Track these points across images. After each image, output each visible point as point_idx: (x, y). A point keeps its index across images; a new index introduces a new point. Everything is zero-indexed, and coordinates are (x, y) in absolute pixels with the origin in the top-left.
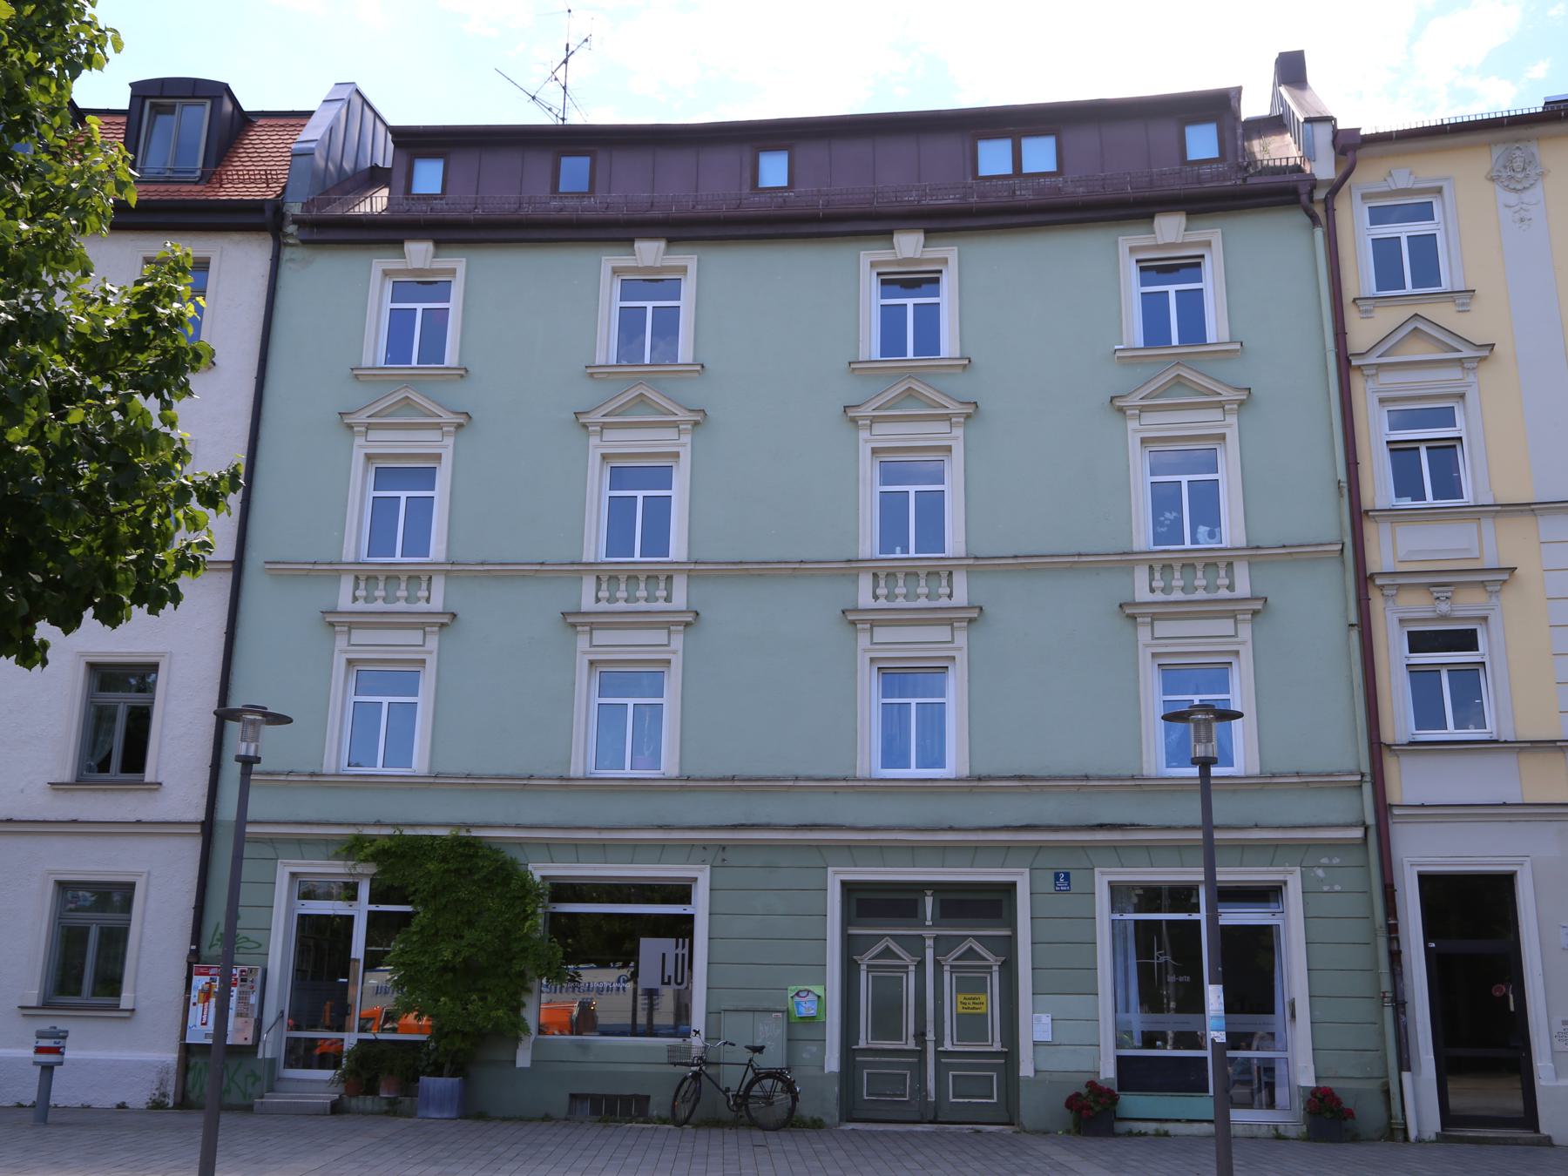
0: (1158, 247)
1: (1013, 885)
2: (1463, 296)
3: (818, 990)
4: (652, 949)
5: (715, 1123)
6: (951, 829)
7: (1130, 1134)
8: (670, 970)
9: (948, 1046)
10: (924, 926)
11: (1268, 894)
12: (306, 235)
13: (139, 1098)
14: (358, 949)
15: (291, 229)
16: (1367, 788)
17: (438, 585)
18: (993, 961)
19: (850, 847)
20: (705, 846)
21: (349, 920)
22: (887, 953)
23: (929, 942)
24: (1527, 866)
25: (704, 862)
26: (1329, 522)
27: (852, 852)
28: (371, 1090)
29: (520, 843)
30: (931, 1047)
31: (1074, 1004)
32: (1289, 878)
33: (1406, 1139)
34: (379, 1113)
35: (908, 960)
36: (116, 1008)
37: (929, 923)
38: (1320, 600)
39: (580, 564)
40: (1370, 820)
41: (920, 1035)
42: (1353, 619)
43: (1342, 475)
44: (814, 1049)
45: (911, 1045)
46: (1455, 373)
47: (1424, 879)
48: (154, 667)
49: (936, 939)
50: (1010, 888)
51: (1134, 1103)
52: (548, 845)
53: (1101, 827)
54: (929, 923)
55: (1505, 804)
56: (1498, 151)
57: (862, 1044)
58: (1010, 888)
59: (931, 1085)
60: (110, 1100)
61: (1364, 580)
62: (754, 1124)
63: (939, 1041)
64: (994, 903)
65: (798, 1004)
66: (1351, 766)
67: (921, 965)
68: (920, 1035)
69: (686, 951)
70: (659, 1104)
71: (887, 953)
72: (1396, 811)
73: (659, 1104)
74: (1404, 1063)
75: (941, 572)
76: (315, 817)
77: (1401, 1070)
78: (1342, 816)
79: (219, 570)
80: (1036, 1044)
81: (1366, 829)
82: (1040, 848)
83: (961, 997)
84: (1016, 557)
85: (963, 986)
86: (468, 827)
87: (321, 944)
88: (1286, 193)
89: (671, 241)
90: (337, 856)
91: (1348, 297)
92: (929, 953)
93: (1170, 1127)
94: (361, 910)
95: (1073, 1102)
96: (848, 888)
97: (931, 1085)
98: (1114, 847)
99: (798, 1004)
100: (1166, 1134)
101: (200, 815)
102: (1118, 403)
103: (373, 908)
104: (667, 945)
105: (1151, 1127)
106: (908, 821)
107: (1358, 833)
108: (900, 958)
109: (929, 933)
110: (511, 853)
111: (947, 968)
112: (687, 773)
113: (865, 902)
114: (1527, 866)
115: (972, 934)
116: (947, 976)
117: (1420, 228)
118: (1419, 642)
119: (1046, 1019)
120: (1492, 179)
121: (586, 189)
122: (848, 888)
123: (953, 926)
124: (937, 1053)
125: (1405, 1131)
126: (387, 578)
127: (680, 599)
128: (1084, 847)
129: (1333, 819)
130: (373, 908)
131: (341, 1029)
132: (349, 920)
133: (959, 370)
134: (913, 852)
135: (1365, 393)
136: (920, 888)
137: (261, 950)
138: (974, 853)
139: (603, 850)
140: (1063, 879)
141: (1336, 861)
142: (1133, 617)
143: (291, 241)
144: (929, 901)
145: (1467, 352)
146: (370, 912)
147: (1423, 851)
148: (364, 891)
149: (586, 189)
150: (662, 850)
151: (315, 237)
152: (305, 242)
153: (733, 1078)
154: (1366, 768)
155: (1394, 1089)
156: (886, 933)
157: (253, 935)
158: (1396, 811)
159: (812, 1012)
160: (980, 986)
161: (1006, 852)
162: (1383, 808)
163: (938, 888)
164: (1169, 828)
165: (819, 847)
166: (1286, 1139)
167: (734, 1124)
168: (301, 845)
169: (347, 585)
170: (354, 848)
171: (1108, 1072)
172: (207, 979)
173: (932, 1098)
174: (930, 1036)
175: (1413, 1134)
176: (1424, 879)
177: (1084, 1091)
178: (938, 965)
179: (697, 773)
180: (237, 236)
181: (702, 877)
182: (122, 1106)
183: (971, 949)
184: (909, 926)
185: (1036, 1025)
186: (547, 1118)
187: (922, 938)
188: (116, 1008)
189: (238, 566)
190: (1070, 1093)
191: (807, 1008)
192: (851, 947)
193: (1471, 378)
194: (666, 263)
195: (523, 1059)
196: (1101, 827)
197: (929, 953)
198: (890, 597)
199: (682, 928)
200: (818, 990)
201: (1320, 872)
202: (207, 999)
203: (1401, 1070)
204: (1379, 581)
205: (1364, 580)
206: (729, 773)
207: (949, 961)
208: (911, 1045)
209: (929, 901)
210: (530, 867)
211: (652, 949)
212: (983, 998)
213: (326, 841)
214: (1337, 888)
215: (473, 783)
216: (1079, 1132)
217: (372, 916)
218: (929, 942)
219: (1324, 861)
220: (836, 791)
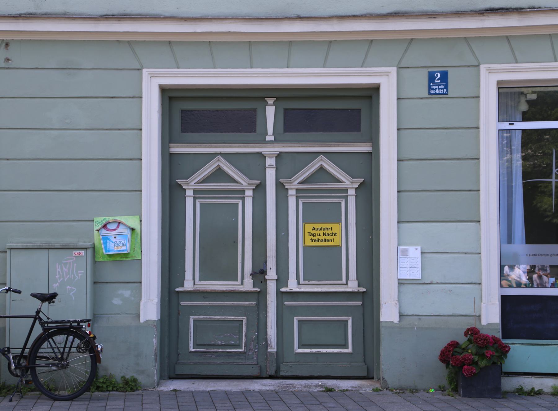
1: (375, 89)
3: (132, 221)
6: (299, 18)
7: (520, 392)
9: (293, 286)
10: (264, 142)
18: (350, 184)
23: (271, 162)
27: (173, 49)
30: (272, 287)
35: (245, 183)
37: (270, 138)
41: (259, 274)
44: (127, 293)
45: (248, 285)
49: (279, 157)
50: (371, 93)
51: (526, 354)
54: (270, 138)
57: (188, 285)
58: (371, 93)
59: (272, 333)
63: (282, 280)
65: (105, 239)
67: (260, 189)
68: (259, 274)
71: (219, 175)
80: (401, 282)
82: (410, 41)
83: (309, 228)
85: (311, 214)
95: (450, 354)
96: (169, 95)
97: (272, 333)
98: (507, 38)
99: (105, 239)
109: (270, 150)
111: (292, 192)
113: (188, 113)
115: (322, 151)
116: (292, 202)
119: (414, 252)
124: (280, 295)
128: (467, 39)
134: (250, 49)
136: (260, 94)
138: (327, 48)
140: (439, 80)
144: (270, 111)
156: (217, 150)
159: (124, 249)
160: (333, 214)
161: (368, 47)
163: (281, 94)
165: (131, 44)
171: (491, 316)
173: (273, 348)
174: (271, 274)
177: (462, 340)
178: (281, 188)
183: (322, 169)
184: (247, 142)
185: (401, 259)
187: (262, 157)
191: (118, 243)
192: (173, 171)
200: (132, 221)
207: (294, 184)
208: (248, 285)
209: (270, 111)
212: (335, 228)
216: (455, 390)
218: (271, 162)
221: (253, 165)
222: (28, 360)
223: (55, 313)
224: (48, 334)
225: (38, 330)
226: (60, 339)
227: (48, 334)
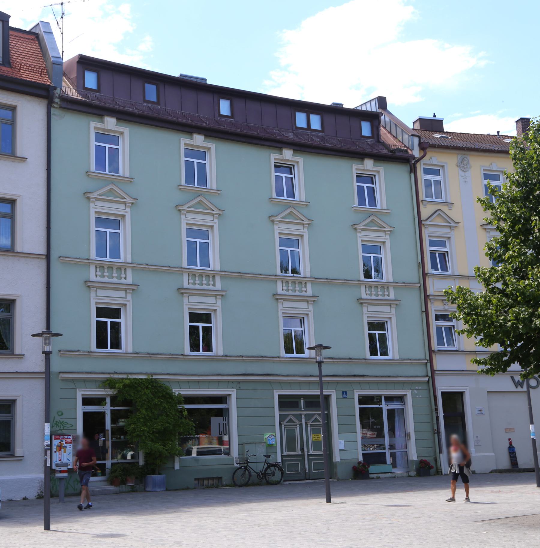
0: (364, 170)
2: (449, 204)
4: (215, 421)
5: (254, 485)
6: (311, 376)
7: (372, 478)
8: (222, 430)
9: (311, 453)
10: (301, 411)
11: (401, 399)
12: (64, 105)
13: (32, 494)
14: (108, 425)
15: (57, 100)
16: (429, 365)
17: (129, 272)
19: (280, 382)
20: (233, 382)
21: (103, 414)
22: (291, 421)
23: (303, 416)
24: (468, 389)
25: (233, 388)
26: (414, 276)
27: (281, 384)
28: (123, 483)
29: (169, 381)
30: (306, 453)
31: (350, 436)
32: (408, 393)
33: (442, 474)
34: (129, 492)
36: (13, 456)
37: (303, 409)
38: (412, 301)
39: (181, 268)
40: (430, 375)
41: (302, 449)
42: (424, 309)
43: (420, 261)
45: (300, 453)
46: (448, 230)
47: (443, 394)
48: (13, 301)
51: (373, 468)
52: (178, 382)
53: (355, 376)
54: (303, 409)
55: (463, 370)
56: (459, 156)
59: (307, 466)
60: (19, 496)
61: (426, 297)
62: (270, 483)
63: (308, 452)
64: (318, 403)
65: (269, 440)
66: (423, 357)
67: (301, 425)
68: (302, 449)
69: (226, 422)
70: (226, 479)
71: (291, 421)
72: (436, 372)
73: (226, 479)
74: (440, 452)
75: (303, 283)
76: (90, 371)
77: (440, 453)
78: (419, 373)
79: (38, 258)
80: (340, 450)
81: (429, 377)
82: (338, 383)
83: (313, 435)
84: (327, 279)
86: (152, 374)
87: (93, 423)
88: (399, 157)
89: (206, 136)
90: (99, 387)
91: (420, 200)
92: (303, 420)
93: (380, 475)
94: (107, 409)
95: (354, 468)
96: (280, 397)
97: (307, 466)
98: (359, 383)
99: (269, 440)
100: (379, 478)
101: (43, 369)
102: (356, 226)
103: (112, 408)
104: (219, 420)
105: (375, 476)
106: (297, 373)
107: (427, 379)
108: (294, 422)
110: (167, 384)
111: (309, 425)
112: (225, 354)
113: (287, 403)
114: (468, 389)
115: (317, 413)
116: (309, 428)
117: (436, 178)
118: (438, 317)
119: (342, 442)
120: (458, 166)
121: (146, 99)
122: (280, 397)
123: (311, 411)
124: (308, 455)
125: (441, 472)
126: (108, 267)
127: (218, 285)
128: (350, 383)
129: (419, 374)
130: (112, 408)
131: (104, 459)
132: (103, 414)
133: (305, 206)
135: (426, 234)
137: (73, 428)
139: (198, 384)
140: (344, 393)
141: (420, 388)
142: (362, 304)
143: (55, 105)
144: (302, 402)
145: (452, 224)
146: (111, 410)
147: (444, 385)
148: (108, 401)
149: (146, 99)
150: (218, 384)
151: (69, 107)
152: (61, 108)
153: (259, 467)
154: (428, 358)
155: (438, 459)
156: (291, 413)
157: (69, 421)
158: (436, 372)
162: (433, 371)
163: (305, 397)
164: (389, 377)
165: (270, 382)
166: (411, 476)
167: (259, 484)
168: (85, 382)
169: (93, 269)
170: (110, 383)
171: (361, 459)
172: (59, 441)
173: (307, 471)
174: (305, 449)
175: (443, 473)
176: (443, 394)
177: (356, 465)
178: (306, 424)
179: (228, 354)
180: (28, 98)
181: (233, 393)
182: (25, 499)
185: (339, 443)
186: (188, 488)
187: (301, 415)
188: (13, 456)
189: (48, 257)
190: (352, 466)
191: (272, 442)
193: (452, 233)
194: (204, 145)
195: (177, 467)
196: (355, 376)
197: (303, 420)
198: (288, 290)
199: (222, 413)
201: (416, 391)
202: (60, 449)
203: (440, 453)
204: (431, 297)
205: (426, 297)
206: (239, 354)
207: (310, 422)
208: (300, 453)
209: (302, 402)
210: (174, 390)
211: (215, 421)
213: (95, 380)
214: (420, 396)
215: (150, 356)
216: (355, 479)
217: (112, 411)
218: (303, 416)
219: (417, 388)
220: (274, 362)
221: (299, 417)
222: (265, 474)
223: (271, 460)
224: (269, 467)
225: (266, 466)
226: (272, 468)
227: (269, 467)
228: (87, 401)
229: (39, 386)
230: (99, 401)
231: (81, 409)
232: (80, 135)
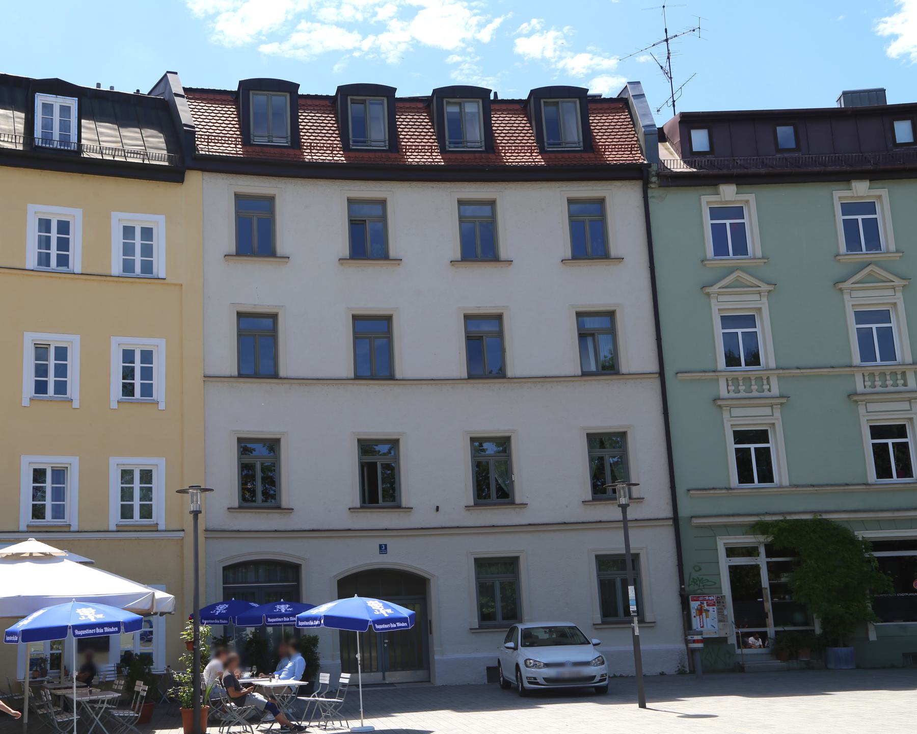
13: (671, 668)
14: (765, 582)
21: (757, 567)
29: (848, 521)
76: (731, 512)
86: (821, 512)
87: (743, 580)
94: (762, 561)
103: (769, 560)
130: (769, 560)
131: (765, 626)
132: (757, 567)
148: (762, 550)
168: (728, 529)
170: (760, 528)
172: (699, 603)
182: (662, 674)
186: (893, 667)
189: (662, 374)
195: (873, 636)
202: (701, 614)
210: (856, 533)
213: (741, 525)
228: (731, 552)
229: (666, 535)
230: (751, 551)
231: (724, 563)
232: (691, 216)
